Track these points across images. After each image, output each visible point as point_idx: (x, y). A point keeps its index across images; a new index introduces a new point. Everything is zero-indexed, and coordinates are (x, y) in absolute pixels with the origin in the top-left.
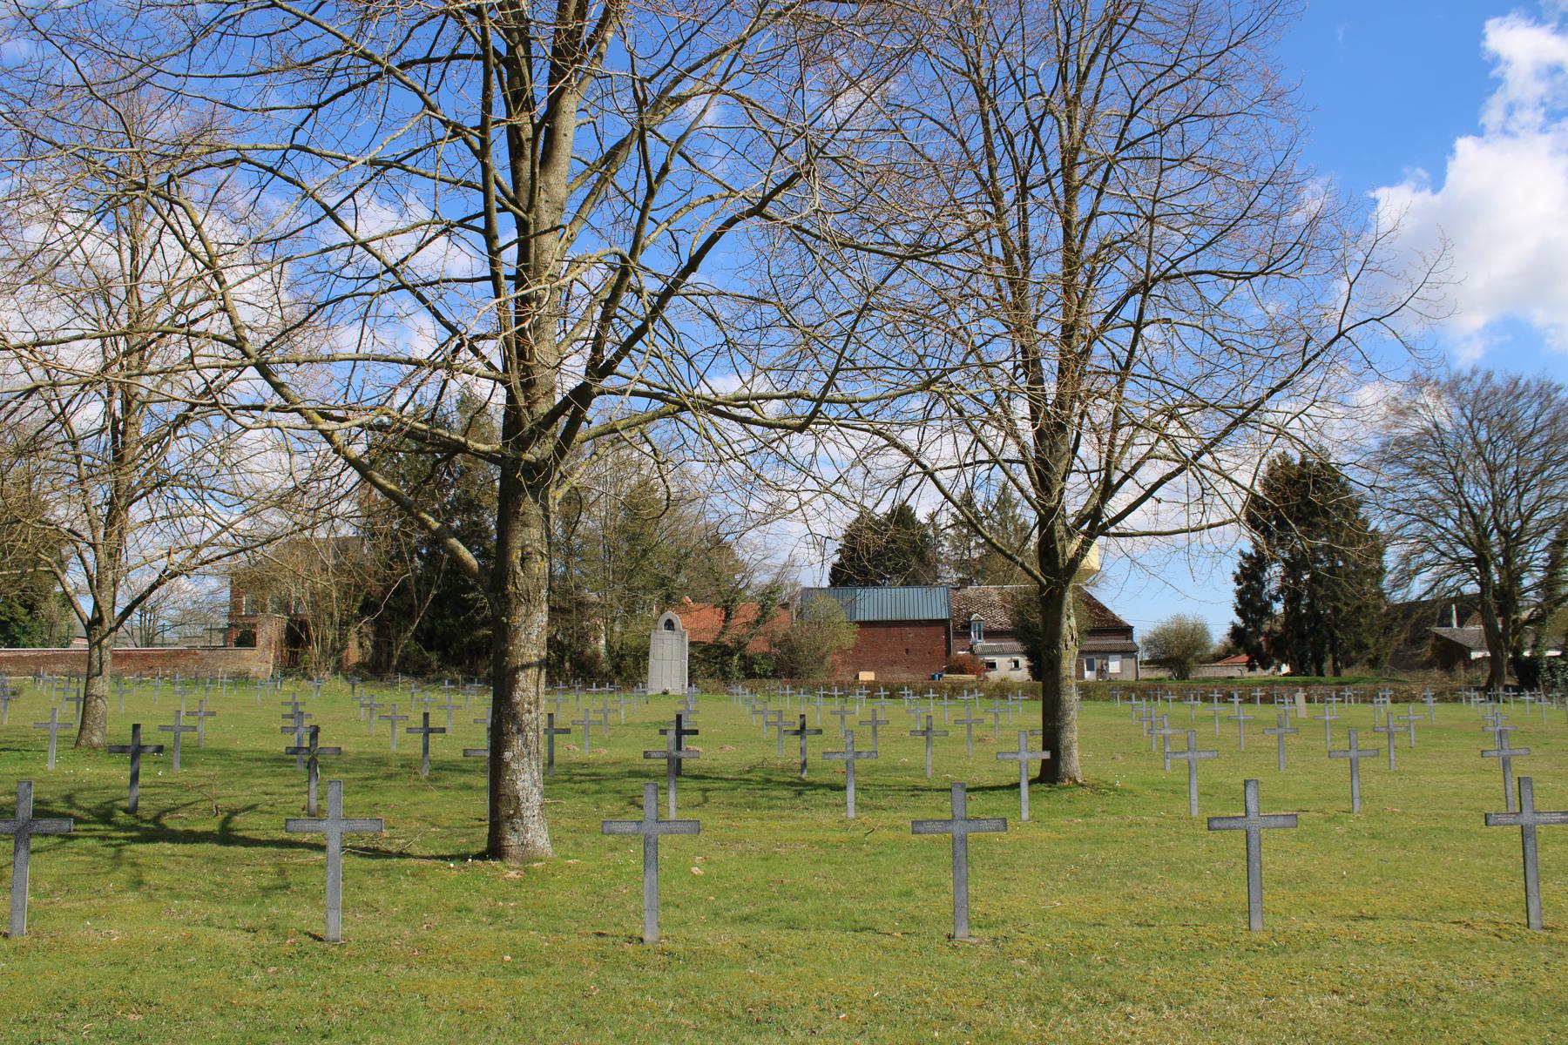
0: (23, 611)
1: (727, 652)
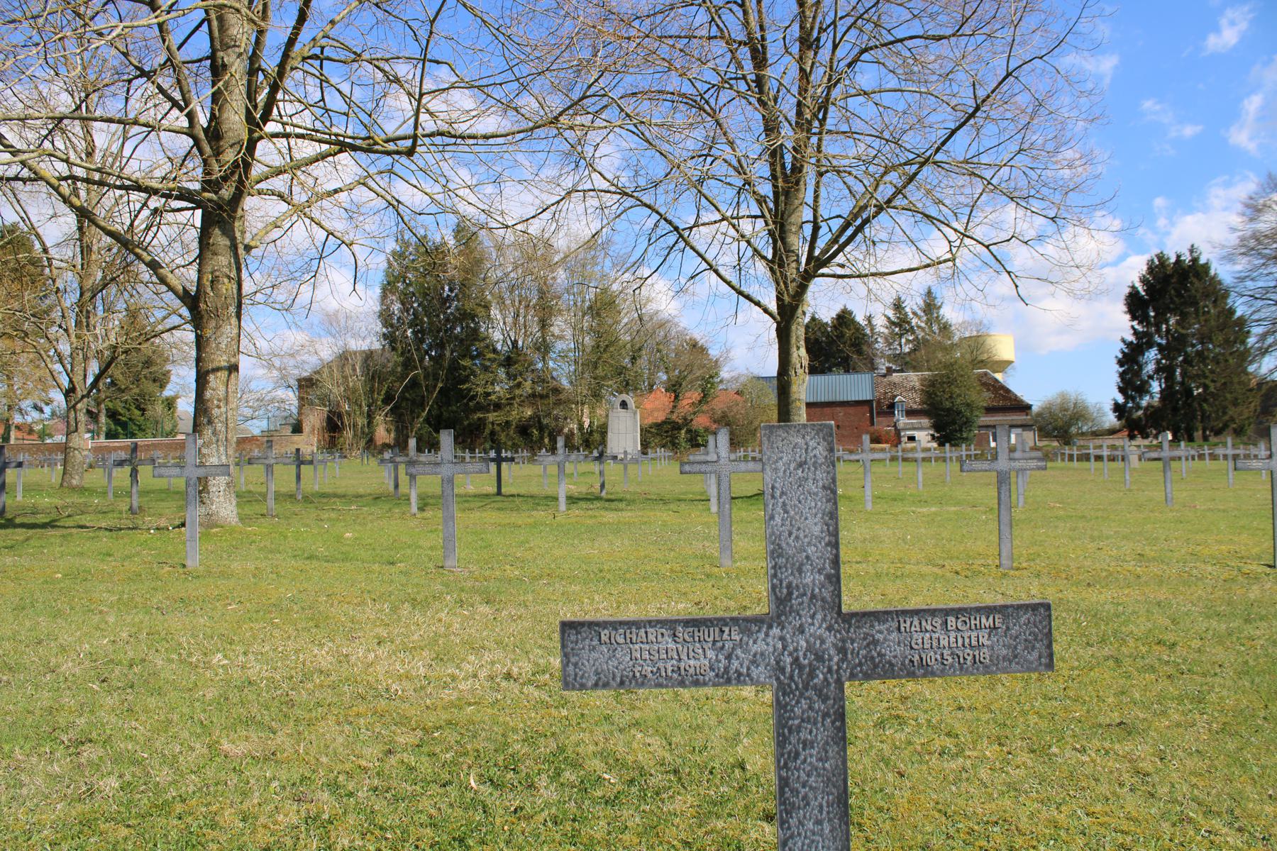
0: (138, 412)
1: (676, 427)
